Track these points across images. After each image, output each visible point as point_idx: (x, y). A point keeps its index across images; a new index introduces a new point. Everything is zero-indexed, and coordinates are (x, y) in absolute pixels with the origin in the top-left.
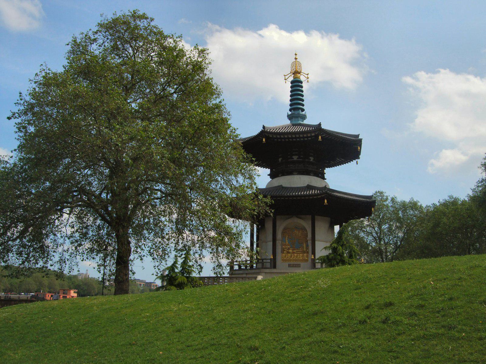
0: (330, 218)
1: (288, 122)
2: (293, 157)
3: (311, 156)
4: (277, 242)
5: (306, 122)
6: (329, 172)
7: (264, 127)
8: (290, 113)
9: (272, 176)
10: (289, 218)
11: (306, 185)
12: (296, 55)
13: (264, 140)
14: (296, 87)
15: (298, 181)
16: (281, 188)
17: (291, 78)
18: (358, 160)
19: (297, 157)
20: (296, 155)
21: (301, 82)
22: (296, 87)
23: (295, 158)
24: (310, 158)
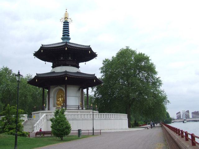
0: (51, 86)
1: (61, 41)
4: (50, 99)
5: (70, 41)
6: (81, 64)
7: (42, 45)
9: (53, 67)
10: (56, 87)
11: (76, 72)
12: (66, 9)
13: (42, 51)
14: (66, 25)
17: (64, 21)
20: (62, 57)
21: (68, 23)
22: (66, 25)
23: (62, 58)
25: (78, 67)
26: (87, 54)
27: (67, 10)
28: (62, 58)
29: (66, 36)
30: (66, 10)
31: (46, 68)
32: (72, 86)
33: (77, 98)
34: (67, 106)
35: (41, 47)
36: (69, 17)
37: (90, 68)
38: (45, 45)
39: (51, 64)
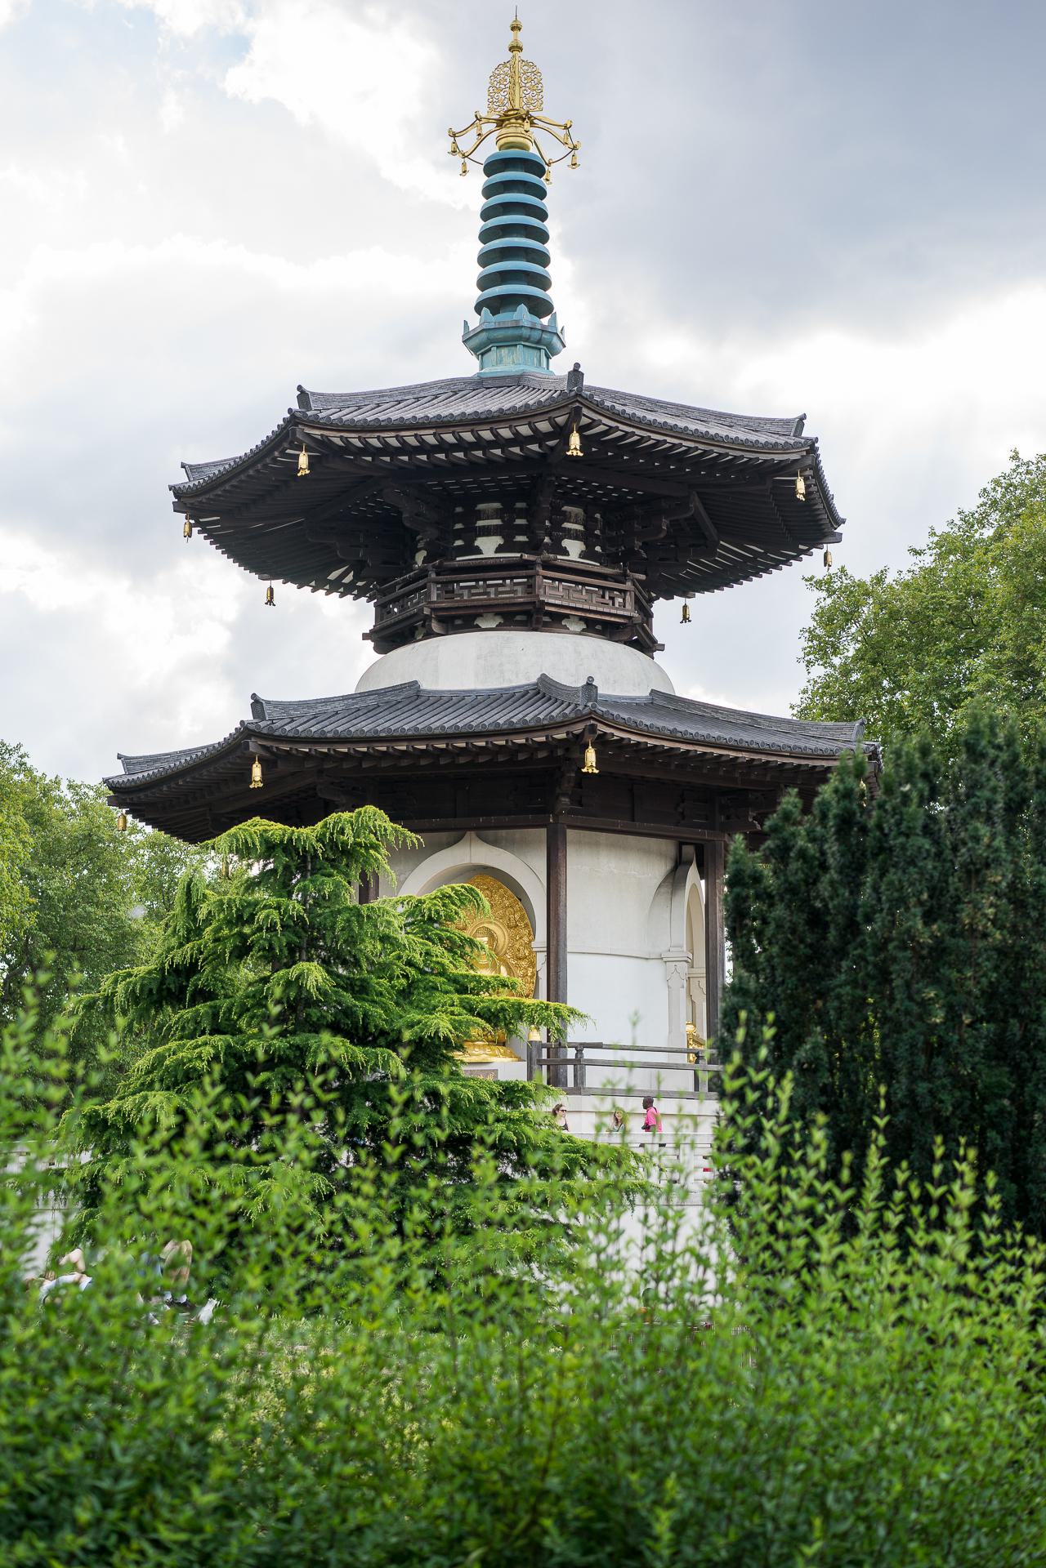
1: (467, 366)
2: (480, 542)
3: (575, 536)
8: (475, 321)
9: (390, 636)
10: (449, 845)
13: (303, 460)
15: (474, 667)
16: (411, 695)
17: (490, 149)
18: (831, 548)
19: (497, 540)
21: (537, 167)
24: (566, 543)
25: (646, 645)
26: (726, 504)
27: (522, 37)
28: (488, 547)
29: (522, 314)
30: (510, 37)
31: (321, 647)
32: (603, 837)
33: (656, 970)
34: (682, 1059)
35: (293, 420)
36: (550, 109)
37: (738, 656)
38: (327, 398)
39: (360, 613)
